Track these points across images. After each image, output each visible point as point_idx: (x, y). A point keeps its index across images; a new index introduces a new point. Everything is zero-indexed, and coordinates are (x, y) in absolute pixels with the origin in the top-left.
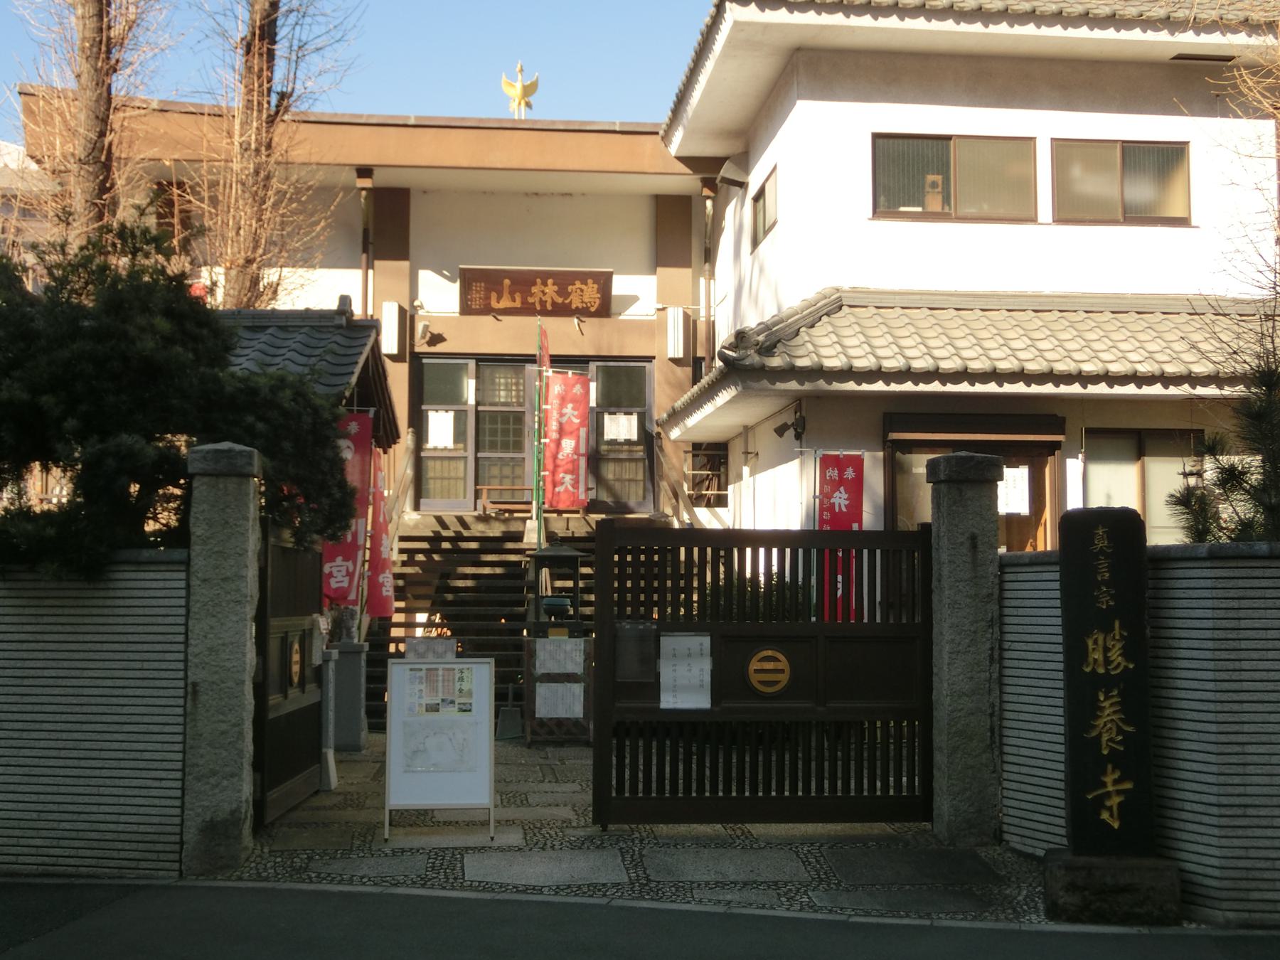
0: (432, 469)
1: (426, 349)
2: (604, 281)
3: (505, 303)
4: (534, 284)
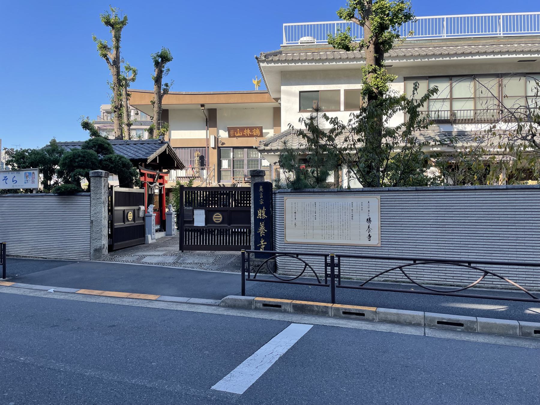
0: (223, 173)
2: (261, 129)
3: (238, 135)
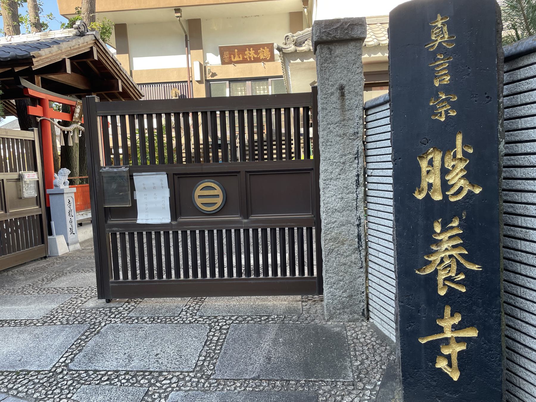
1: (210, 78)
3: (237, 59)
4: (246, 50)
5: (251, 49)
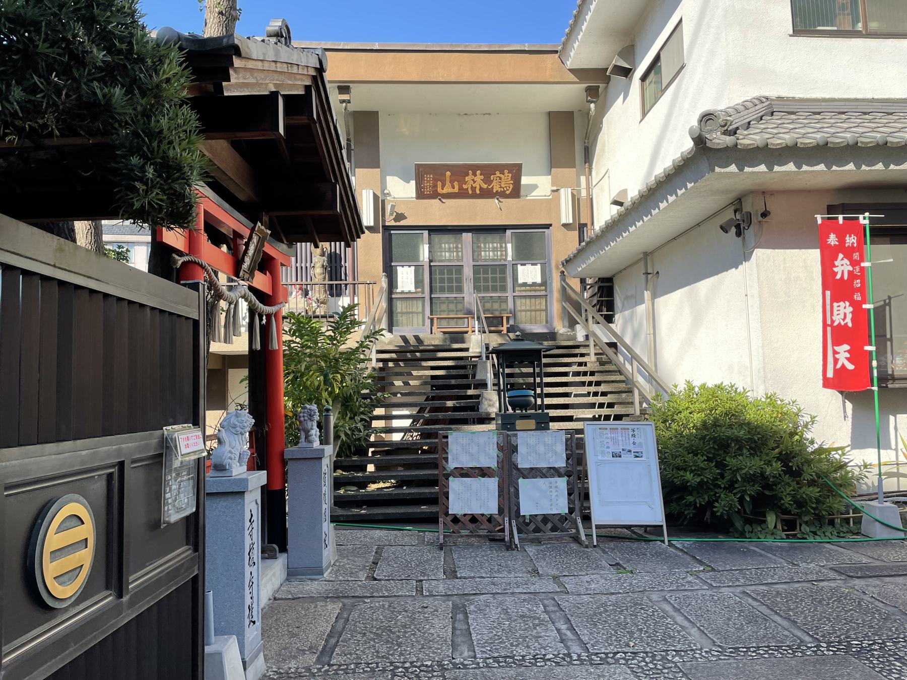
0: (399, 306)
1: (393, 223)
2: (516, 171)
3: (447, 189)
4: (468, 175)
5: (478, 172)
